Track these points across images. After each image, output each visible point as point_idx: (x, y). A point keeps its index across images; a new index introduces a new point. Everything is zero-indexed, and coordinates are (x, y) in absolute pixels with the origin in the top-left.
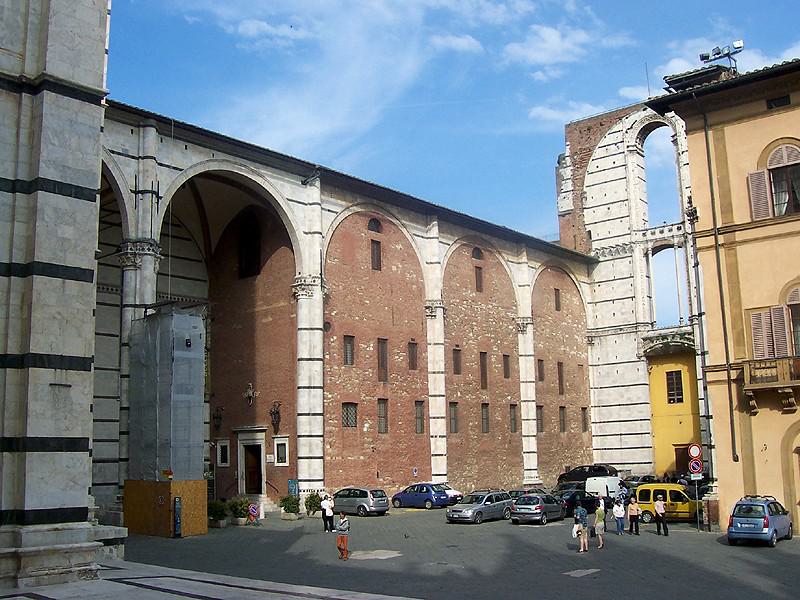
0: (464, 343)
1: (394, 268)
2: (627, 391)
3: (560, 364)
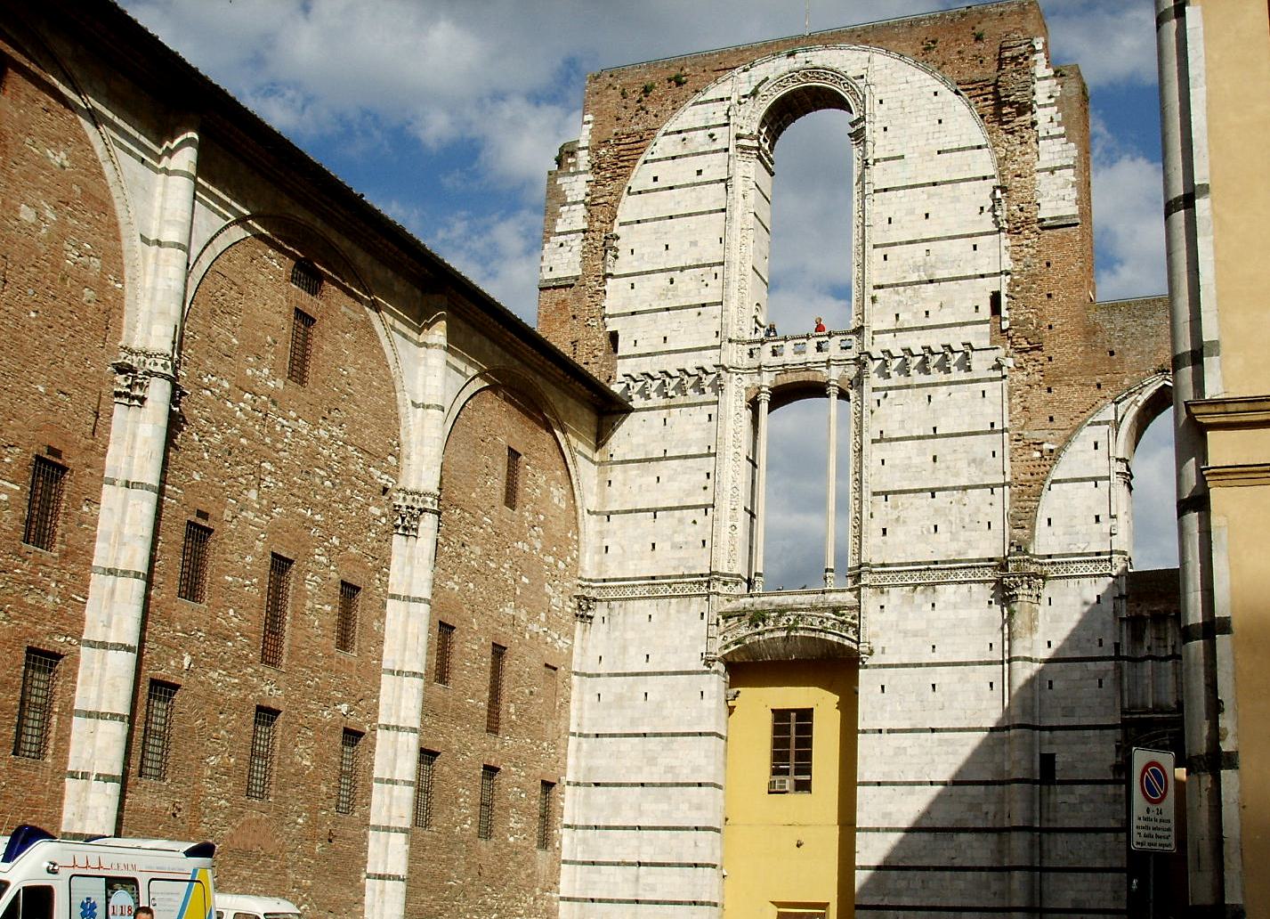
0: (227, 514)
3: (498, 651)
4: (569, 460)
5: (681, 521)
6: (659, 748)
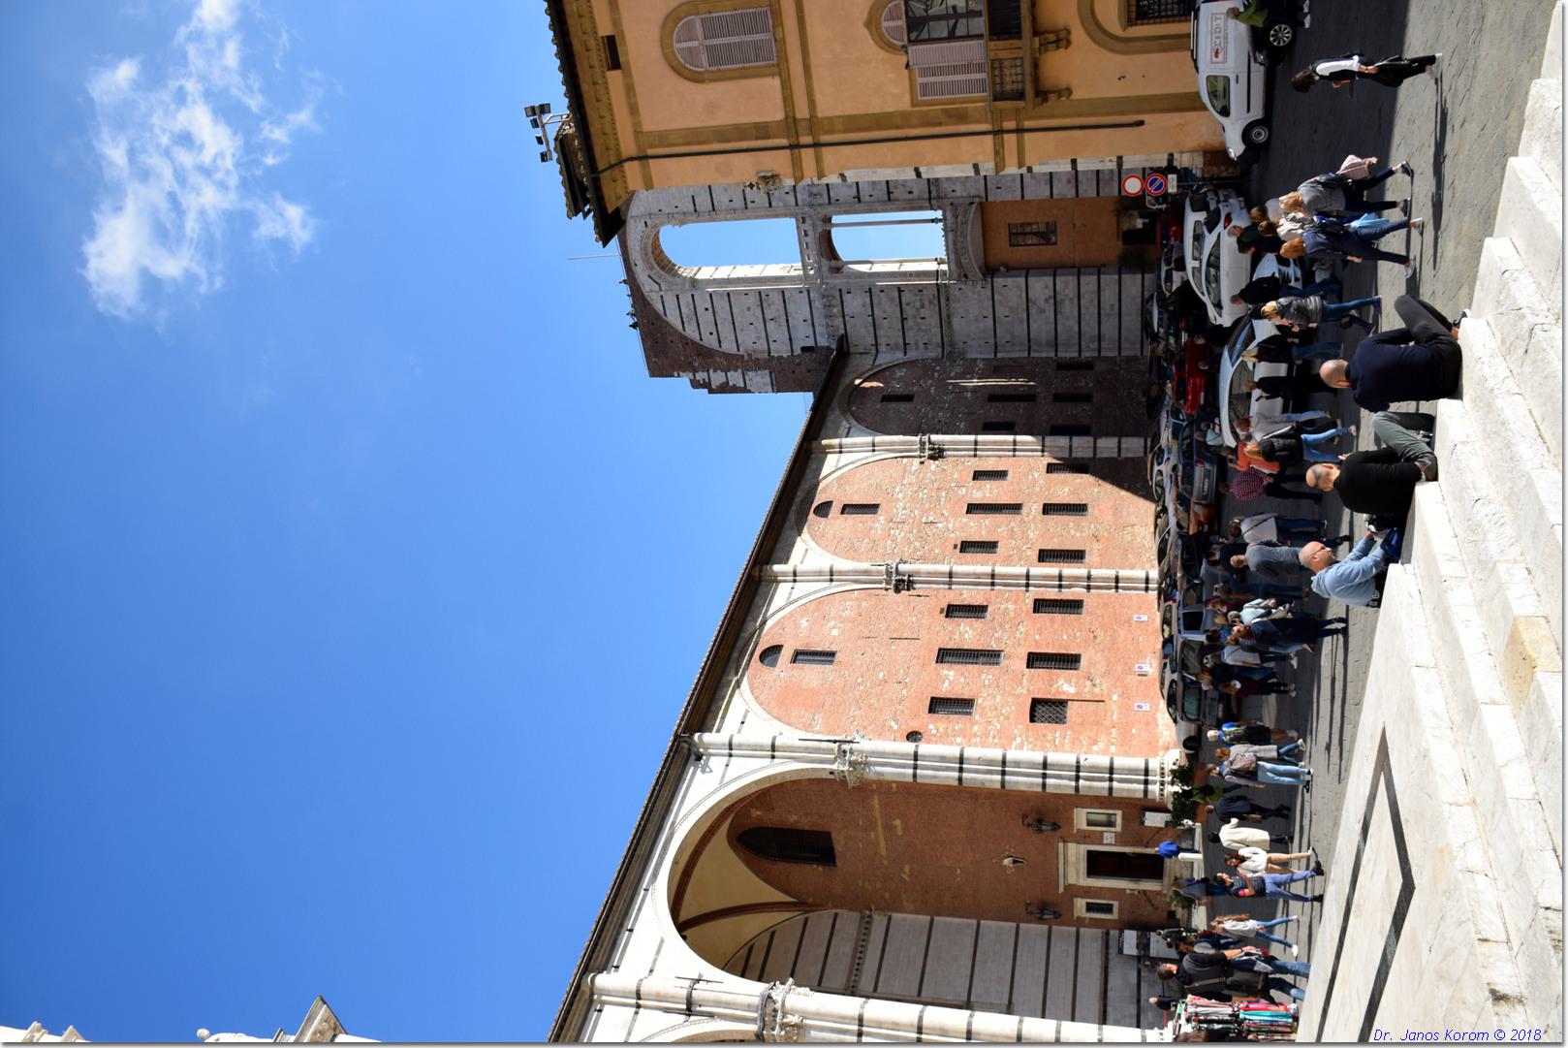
0: (952, 535)
1: (835, 632)
2: (1034, 303)
4: (880, 368)
5: (908, 304)
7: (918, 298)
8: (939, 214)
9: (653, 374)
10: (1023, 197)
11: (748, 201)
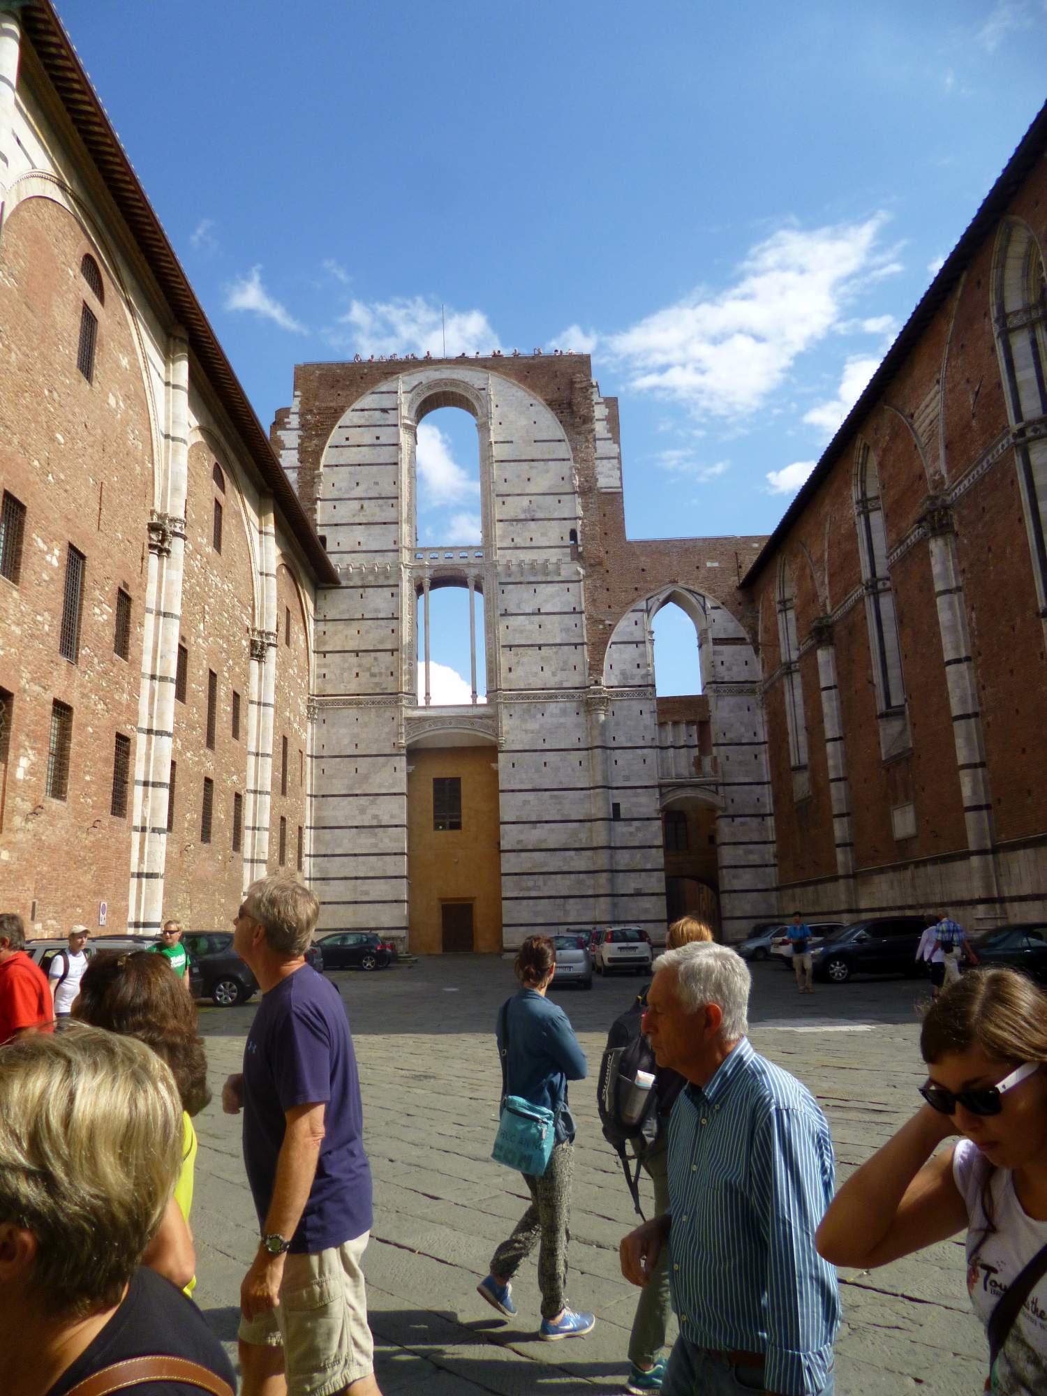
2: (373, 803)
5: (376, 659)
6: (367, 803)
7: (383, 671)
8: (482, 700)
9: (298, 369)
10: (503, 791)
11: (505, 499)
